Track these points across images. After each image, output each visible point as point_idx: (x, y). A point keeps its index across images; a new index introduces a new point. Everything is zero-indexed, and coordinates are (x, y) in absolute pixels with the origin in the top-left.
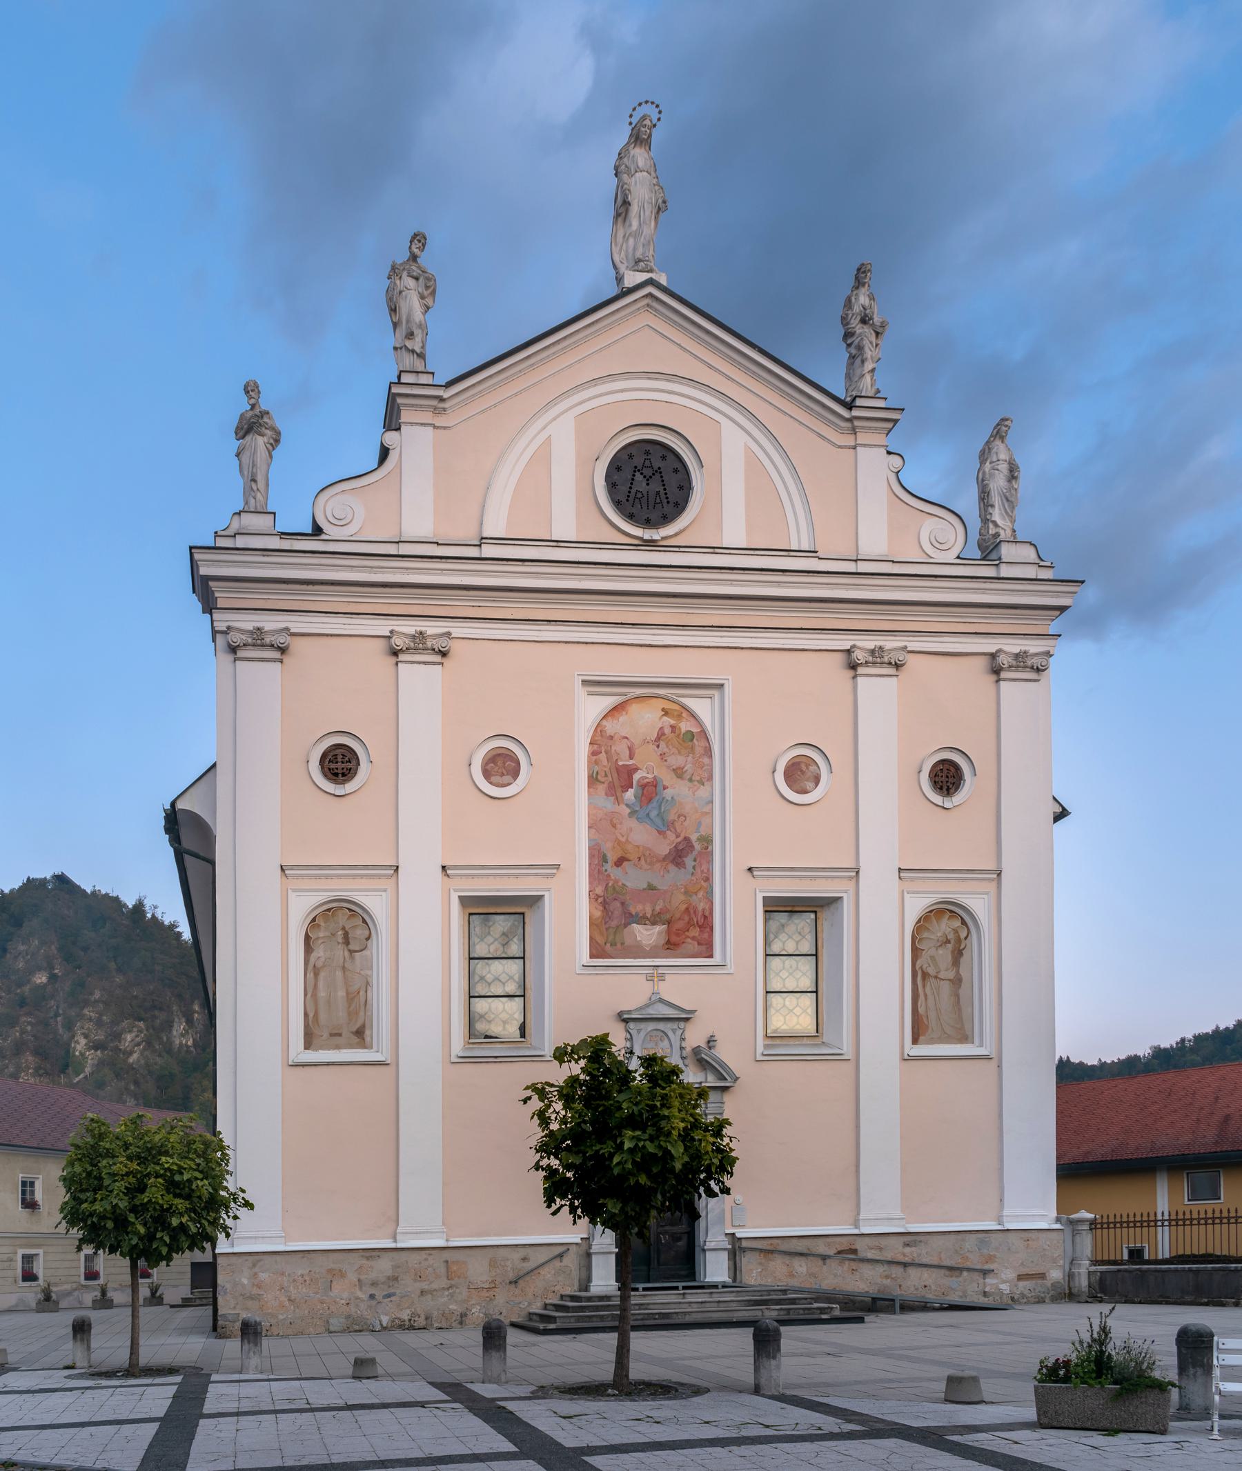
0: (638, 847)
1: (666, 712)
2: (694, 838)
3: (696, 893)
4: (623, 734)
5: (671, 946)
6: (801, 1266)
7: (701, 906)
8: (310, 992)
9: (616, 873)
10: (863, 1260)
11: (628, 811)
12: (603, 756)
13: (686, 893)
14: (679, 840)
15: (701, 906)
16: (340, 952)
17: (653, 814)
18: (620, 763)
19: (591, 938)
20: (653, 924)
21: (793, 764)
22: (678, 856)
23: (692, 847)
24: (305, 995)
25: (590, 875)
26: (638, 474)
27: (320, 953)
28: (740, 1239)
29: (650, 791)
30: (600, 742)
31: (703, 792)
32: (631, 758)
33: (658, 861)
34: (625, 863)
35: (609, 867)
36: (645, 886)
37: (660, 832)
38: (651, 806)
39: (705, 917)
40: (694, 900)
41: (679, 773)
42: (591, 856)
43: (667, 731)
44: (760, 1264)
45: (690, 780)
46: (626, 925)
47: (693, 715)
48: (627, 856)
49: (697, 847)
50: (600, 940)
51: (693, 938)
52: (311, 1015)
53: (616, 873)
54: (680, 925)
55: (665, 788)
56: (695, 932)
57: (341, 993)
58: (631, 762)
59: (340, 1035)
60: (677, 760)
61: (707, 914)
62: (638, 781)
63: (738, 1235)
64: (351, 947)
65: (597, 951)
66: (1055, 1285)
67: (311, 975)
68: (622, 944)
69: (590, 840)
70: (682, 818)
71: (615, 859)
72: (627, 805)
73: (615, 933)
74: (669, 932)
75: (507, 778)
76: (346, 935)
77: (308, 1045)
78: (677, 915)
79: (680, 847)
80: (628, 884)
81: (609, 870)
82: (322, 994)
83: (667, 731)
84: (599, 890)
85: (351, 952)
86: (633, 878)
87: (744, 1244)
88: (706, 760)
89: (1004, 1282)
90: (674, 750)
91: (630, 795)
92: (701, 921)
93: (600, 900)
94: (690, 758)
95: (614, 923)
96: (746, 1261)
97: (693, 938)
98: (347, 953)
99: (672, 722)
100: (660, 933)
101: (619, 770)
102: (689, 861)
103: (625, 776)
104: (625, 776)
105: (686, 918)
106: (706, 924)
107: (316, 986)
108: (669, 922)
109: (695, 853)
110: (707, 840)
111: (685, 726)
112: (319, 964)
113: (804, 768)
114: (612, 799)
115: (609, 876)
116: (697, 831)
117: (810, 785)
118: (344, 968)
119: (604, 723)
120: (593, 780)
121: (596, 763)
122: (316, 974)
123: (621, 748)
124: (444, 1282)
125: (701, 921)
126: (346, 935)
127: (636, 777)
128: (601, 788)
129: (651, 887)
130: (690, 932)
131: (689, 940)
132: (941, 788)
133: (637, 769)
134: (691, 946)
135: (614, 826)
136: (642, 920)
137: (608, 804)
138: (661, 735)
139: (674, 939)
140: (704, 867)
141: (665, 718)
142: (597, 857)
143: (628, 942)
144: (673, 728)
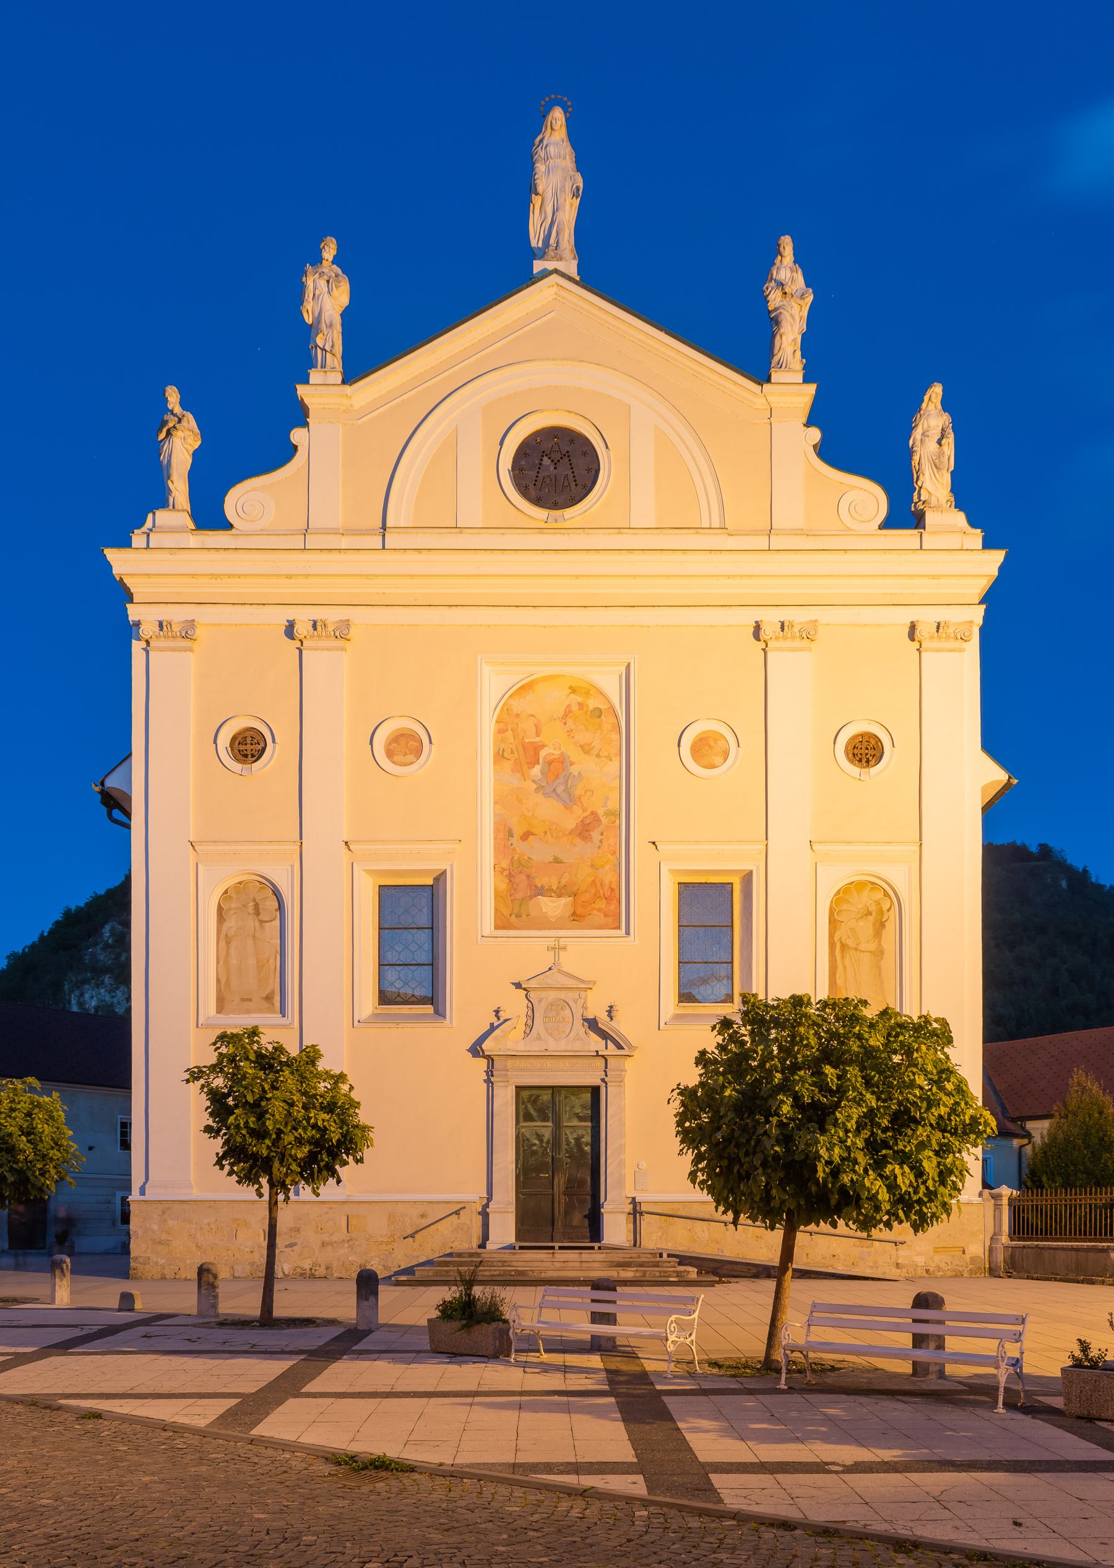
0: (544, 821)
1: (573, 690)
2: (601, 812)
3: (603, 867)
5: (577, 918)
7: (609, 878)
8: (223, 960)
9: (521, 847)
11: (535, 786)
12: (509, 734)
14: (586, 814)
16: (251, 922)
17: (560, 789)
19: (496, 910)
21: (701, 740)
22: (584, 830)
23: (599, 821)
24: (218, 963)
25: (495, 849)
26: (545, 458)
27: (231, 923)
29: (558, 768)
30: (507, 720)
34: (531, 838)
35: (515, 840)
36: (551, 860)
37: (566, 808)
39: (612, 890)
41: (586, 749)
42: (497, 831)
43: (575, 708)
45: (598, 756)
46: (531, 898)
48: (533, 830)
50: (506, 911)
51: (599, 910)
52: (223, 981)
53: (521, 847)
54: (587, 897)
56: (601, 904)
57: (252, 961)
58: (538, 739)
59: (250, 1000)
61: (614, 886)
62: (545, 758)
64: (261, 917)
65: (502, 923)
66: (973, 1260)
67: (223, 944)
68: (528, 915)
69: (495, 815)
72: (534, 781)
73: (520, 905)
74: (575, 904)
75: (411, 758)
76: (257, 907)
77: (220, 1010)
79: (587, 821)
82: (234, 961)
83: (575, 708)
84: (505, 864)
85: (261, 922)
86: (538, 852)
89: (919, 1254)
91: (536, 771)
93: (506, 873)
96: (646, 1222)
97: (599, 910)
98: (257, 923)
99: (580, 699)
100: (565, 905)
101: (525, 747)
102: (595, 835)
104: (532, 753)
105: (593, 891)
107: (228, 953)
109: (602, 827)
111: (592, 703)
112: (231, 933)
113: (712, 743)
115: (514, 849)
116: (605, 805)
117: (718, 760)
118: (254, 936)
120: (499, 756)
121: (503, 740)
122: (228, 943)
126: (257, 907)
127: (543, 753)
128: (508, 765)
129: (557, 861)
131: (595, 912)
132: (860, 760)
133: (544, 746)
134: (599, 918)
135: (520, 801)
138: (568, 712)
139: (579, 911)
141: (572, 696)
142: (504, 834)
144: (581, 705)
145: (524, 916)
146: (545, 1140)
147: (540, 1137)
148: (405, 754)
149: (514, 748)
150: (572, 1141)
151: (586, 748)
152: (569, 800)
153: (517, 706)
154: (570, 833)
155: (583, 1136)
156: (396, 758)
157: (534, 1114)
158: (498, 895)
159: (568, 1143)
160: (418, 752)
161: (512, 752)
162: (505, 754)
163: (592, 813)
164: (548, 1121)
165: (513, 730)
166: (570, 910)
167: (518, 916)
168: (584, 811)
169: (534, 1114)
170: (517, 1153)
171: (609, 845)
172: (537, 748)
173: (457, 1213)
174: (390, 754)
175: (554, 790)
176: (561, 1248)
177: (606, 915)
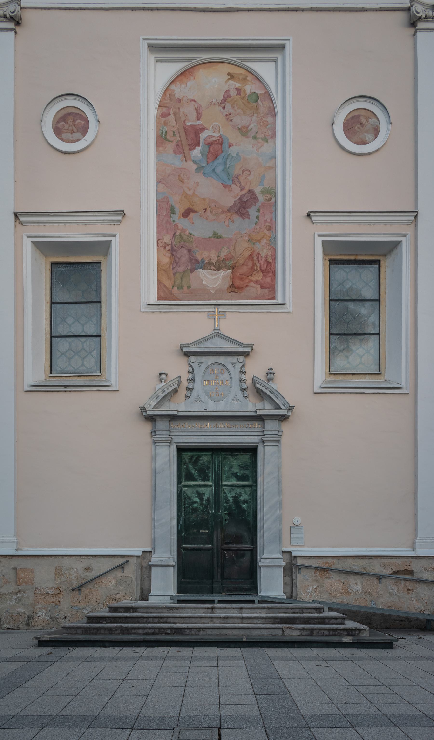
0: (204, 199)
1: (232, 76)
2: (257, 190)
3: (259, 241)
4: (191, 97)
6: (356, 585)
10: (418, 581)
11: (195, 167)
12: (171, 118)
13: (250, 240)
14: (243, 192)
15: (263, 253)
17: (219, 170)
18: (188, 124)
20: (218, 269)
21: (353, 118)
22: (242, 208)
23: (256, 198)
28: (295, 557)
30: (168, 104)
31: (266, 148)
32: (198, 119)
33: (223, 212)
34: (192, 214)
35: (176, 217)
36: (211, 235)
37: (225, 186)
38: (216, 162)
39: (268, 263)
40: (258, 247)
41: (244, 131)
42: (159, 208)
43: (233, 93)
44: (316, 581)
45: (255, 138)
46: (192, 270)
47: (258, 78)
48: (193, 208)
49: (261, 199)
50: (168, 283)
51: (256, 282)
53: (183, 223)
54: (245, 270)
55: (230, 146)
56: (258, 276)
58: (198, 123)
60: (241, 120)
61: (270, 260)
62: (205, 140)
63: (294, 554)
68: (189, 287)
69: (158, 193)
70: (247, 173)
71: (182, 210)
72: (195, 162)
73: (182, 278)
74: (233, 276)
78: (242, 261)
79: (245, 199)
80: (195, 233)
81: (177, 221)
83: (233, 93)
84: (167, 239)
86: (199, 228)
87: (300, 562)
88: (270, 119)
90: (239, 111)
91: (197, 152)
92: (264, 267)
93: (168, 248)
94: (254, 118)
95: (181, 269)
96: (301, 578)
97: (256, 282)
99: (238, 85)
100: (224, 278)
102: (253, 212)
103: (193, 135)
104: (193, 135)
105: (250, 264)
106: (268, 269)
108: (233, 268)
109: (258, 204)
110: (270, 193)
111: (249, 89)
113: (363, 120)
114: (180, 156)
115: (176, 226)
117: (369, 136)
119: (173, 87)
120: (162, 139)
121: (165, 124)
123: (189, 111)
124: (12, 587)
125: (264, 267)
127: (203, 136)
128: (170, 147)
129: (216, 236)
130: (253, 276)
131: (252, 284)
133: (204, 129)
134: (255, 289)
135: (182, 181)
136: (208, 265)
137: (177, 161)
138: (227, 97)
139: (238, 283)
140: (268, 218)
141: (231, 82)
142: (165, 209)
143: (194, 285)
144: (238, 90)
145: (185, 288)
146: (205, 498)
147: (200, 496)
148: (73, 132)
149: (175, 130)
150: (231, 499)
151: (244, 130)
152: (230, 180)
153: (178, 90)
154: (229, 210)
155: (240, 495)
156: (63, 136)
157: (195, 474)
158: (160, 268)
159: (227, 501)
160: (84, 130)
161: (174, 135)
162: (168, 137)
163: (250, 191)
164: (208, 480)
165: (175, 114)
166: (227, 285)
167: (180, 287)
168: (242, 190)
169: (195, 474)
170: (179, 511)
171: (265, 221)
172: (197, 131)
173: (121, 567)
174: (58, 132)
175: (214, 170)
176: (220, 602)
177: (262, 287)
